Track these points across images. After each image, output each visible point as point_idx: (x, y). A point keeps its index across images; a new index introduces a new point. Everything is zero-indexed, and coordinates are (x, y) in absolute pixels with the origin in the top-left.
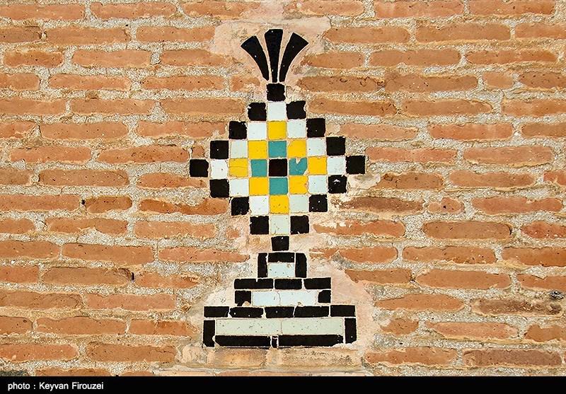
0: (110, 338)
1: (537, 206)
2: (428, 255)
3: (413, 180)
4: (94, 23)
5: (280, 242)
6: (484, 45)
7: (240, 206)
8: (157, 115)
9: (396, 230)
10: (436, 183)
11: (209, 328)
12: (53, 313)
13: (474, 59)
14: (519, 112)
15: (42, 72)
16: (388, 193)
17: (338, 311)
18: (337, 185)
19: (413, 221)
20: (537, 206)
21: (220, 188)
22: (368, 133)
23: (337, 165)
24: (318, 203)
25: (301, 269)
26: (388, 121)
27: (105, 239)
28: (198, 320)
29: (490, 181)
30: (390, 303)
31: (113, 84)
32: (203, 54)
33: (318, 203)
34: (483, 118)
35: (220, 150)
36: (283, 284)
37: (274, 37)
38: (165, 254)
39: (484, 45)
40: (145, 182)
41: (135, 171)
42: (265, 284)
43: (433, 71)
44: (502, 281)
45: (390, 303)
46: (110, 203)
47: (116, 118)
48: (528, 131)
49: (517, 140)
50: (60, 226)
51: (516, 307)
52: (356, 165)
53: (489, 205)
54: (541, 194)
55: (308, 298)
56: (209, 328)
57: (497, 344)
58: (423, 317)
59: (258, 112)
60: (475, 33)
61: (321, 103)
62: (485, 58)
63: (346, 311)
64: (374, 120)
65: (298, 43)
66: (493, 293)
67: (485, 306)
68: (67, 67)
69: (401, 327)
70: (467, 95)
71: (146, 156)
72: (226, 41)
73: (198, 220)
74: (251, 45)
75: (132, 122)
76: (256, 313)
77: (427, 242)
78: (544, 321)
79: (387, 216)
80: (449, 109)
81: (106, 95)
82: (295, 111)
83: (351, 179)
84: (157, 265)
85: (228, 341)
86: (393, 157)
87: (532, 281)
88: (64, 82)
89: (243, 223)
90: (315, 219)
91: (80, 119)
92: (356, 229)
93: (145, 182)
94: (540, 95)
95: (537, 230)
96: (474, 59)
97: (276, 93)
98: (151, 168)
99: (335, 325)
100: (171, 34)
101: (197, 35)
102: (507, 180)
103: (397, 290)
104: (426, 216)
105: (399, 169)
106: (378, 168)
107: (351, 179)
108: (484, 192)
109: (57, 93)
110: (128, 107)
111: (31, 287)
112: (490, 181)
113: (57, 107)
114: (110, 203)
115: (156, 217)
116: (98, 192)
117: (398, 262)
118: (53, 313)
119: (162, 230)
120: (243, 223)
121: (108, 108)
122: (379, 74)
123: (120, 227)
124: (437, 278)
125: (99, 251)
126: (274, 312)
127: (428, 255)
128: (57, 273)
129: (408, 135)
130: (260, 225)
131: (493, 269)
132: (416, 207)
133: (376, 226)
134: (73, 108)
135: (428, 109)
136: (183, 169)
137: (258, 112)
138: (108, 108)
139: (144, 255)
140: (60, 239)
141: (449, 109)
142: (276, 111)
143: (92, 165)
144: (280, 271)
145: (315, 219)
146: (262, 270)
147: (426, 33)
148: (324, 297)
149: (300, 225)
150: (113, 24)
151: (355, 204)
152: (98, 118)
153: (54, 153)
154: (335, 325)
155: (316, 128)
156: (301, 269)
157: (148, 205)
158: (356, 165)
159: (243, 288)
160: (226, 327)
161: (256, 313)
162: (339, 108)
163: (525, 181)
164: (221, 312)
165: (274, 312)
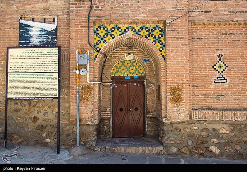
0: (206, 82)
1: (243, 70)
2: (233, 75)
3: (232, 68)
4: (203, 53)
5: (221, 74)
6: (238, 56)
7: (217, 70)
8: (209, 62)
9: (231, 72)
10: (234, 68)
11: (214, 81)
12: (200, 80)
13: (237, 57)
14: (241, 62)
15: (199, 58)
16: (230, 69)
17: (226, 80)
18: (226, 68)
19: (232, 72)
20: (243, 70)
21: (215, 69)
22: (228, 64)
23: (225, 67)
24: (224, 70)
25: (222, 76)
26: (230, 62)
27: (205, 73)
28: (213, 81)
29: (238, 68)
30: (230, 79)
31: (205, 59)
32: (213, 56)
33: (224, 70)
34: (238, 62)
35: (215, 65)
36: (221, 77)
37: (220, 55)
38: (210, 75)
39: (238, 56)
40: (208, 68)
41: (207, 67)
42: (219, 77)
43: (234, 58)
44: (240, 77)
45: (230, 79)
46: (205, 70)
47: (205, 62)
48: (242, 63)
49: (241, 64)
50: (201, 72)
51: (241, 79)
52: (227, 67)
53: (239, 70)
54: (243, 69)
55: (223, 79)
56: (214, 81)
57: (239, 82)
58: (233, 80)
59: (218, 62)
60: (237, 54)
61: (224, 61)
62: (238, 57)
63: (227, 80)
64: (228, 62)
65: (222, 55)
66: (239, 78)
67: (238, 79)
68: (201, 57)
69: (231, 81)
70: (237, 60)
71: (208, 66)
72: (215, 55)
73: (213, 72)
74: (218, 56)
75: (207, 63)
76: (219, 80)
77: (233, 73)
78: (243, 80)
79: (230, 71)
80: (235, 61)
81: (204, 60)
82: (222, 62)
83: (227, 68)
84: (210, 76)
85: (216, 82)
86: (230, 66)
87: (242, 77)
88: (201, 59)
89: (217, 72)
90: (224, 71)
91: (202, 62)
92: (227, 72)
93: (208, 68)
94: (243, 60)
95: (243, 72)
96: (237, 57)
97: (220, 60)
98: (209, 67)
99: (226, 81)
100: (210, 54)
101: (212, 55)
102: (240, 68)
103: (230, 78)
104: (233, 71)
105: (231, 67)
106: (229, 67)
107: (227, 68)
108: (238, 69)
109: (200, 60)
110: (207, 61)
111: (198, 78)
112: (238, 68)
113: (200, 61)
114: (205, 70)
115: (209, 71)
116: (204, 69)
117: (231, 75)
118: (200, 80)
119: (210, 73)
120: (217, 72)
121: (204, 61)
122: (229, 58)
123: (206, 72)
124: (234, 77)
125: (204, 75)
126: (220, 80)
127: (233, 75)
128: (201, 77)
129: (232, 64)
130: (219, 72)
131: (239, 76)
132: (232, 70)
133: (229, 72)
134: (202, 61)
135: (233, 61)
136: (212, 67)
137: (218, 62)
138: (204, 61)
139: (208, 75)
140: (201, 73)
141: (235, 61)
142: (220, 62)
143: (204, 67)
144: (220, 76)
145: (224, 71)
146: (219, 76)
147: (233, 54)
148: (224, 78)
149: (222, 72)
150: (205, 53)
151: (227, 70)
152: (204, 62)
153: (200, 66)
154: (226, 81)
155: (224, 63)
156: (222, 76)
157: (209, 70)
158: (227, 67)
159: (217, 78)
160: (216, 81)
161: (219, 80)
162: (225, 61)
163: (242, 68)
164: (215, 80)
165: (220, 80)
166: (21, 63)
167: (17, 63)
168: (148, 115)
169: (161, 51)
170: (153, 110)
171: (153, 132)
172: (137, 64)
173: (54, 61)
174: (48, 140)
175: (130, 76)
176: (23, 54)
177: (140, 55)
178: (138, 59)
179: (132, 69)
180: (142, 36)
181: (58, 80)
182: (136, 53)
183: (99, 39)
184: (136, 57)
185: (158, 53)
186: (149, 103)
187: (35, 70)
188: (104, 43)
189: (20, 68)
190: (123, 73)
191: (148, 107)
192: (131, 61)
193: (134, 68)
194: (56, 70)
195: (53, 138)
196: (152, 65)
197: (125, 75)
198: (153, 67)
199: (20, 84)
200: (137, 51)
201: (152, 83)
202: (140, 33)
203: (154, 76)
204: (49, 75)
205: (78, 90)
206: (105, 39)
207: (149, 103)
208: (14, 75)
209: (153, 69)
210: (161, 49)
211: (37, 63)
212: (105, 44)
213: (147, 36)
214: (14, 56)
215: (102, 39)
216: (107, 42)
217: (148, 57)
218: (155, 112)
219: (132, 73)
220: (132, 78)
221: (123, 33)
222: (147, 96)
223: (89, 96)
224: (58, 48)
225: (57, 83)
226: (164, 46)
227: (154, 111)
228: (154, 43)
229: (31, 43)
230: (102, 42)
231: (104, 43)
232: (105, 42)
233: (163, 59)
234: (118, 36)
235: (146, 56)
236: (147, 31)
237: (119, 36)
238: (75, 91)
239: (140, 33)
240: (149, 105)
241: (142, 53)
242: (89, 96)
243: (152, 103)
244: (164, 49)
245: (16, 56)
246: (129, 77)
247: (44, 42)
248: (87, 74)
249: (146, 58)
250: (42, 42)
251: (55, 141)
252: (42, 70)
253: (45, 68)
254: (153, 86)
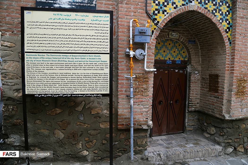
166: (46, 36)
167: (40, 36)
168: (191, 108)
169: (227, 32)
170: (196, 102)
171: (192, 127)
172: (179, 45)
173: (102, 35)
174: (85, 153)
175: (172, 60)
176: (51, 21)
177: (186, 35)
178: (184, 39)
179: (174, 52)
180: (209, 10)
181: (109, 67)
182: (181, 32)
183: (157, 7)
184: (181, 36)
185: (225, 35)
186: (193, 94)
187: (71, 49)
188: (163, 13)
189: (44, 45)
190: (164, 56)
191: (191, 99)
192: (173, 40)
193: (177, 50)
194: (106, 50)
195: (91, 149)
196: (198, 48)
197: (166, 59)
198: (199, 51)
199: (46, 71)
200: (183, 29)
201: (196, 71)
202: (206, 6)
203: (199, 62)
204: (94, 57)
205: (132, 81)
206: (165, 8)
207: (193, 94)
208: (35, 57)
209: (199, 53)
210: (228, 30)
211: (74, 37)
212: (165, 15)
213: (214, 12)
214: (35, 24)
215: (161, 8)
216: (167, 13)
217: (194, 38)
218: (198, 104)
219: (175, 56)
220: (174, 62)
221: (187, 4)
222: (191, 86)
223: (145, 89)
224: (109, 15)
225: (107, 71)
226: (231, 26)
227: (198, 103)
228: (221, 21)
229: (55, 4)
230: (161, 12)
231: (163, 13)
232: (165, 13)
233: (229, 43)
234: (180, 6)
235: (192, 36)
236: (214, 5)
237: (183, 7)
238: (125, 82)
239: (206, 6)
240: (193, 96)
241: (187, 32)
242: (145, 89)
243: (196, 94)
244: (231, 30)
245: (37, 24)
246: (171, 61)
247: (77, 4)
248: (144, 59)
249: (192, 38)
250: (73, 4)
251: (95, 153)
252: (82, 49)
253: (88, 46)
254: (198, 74)
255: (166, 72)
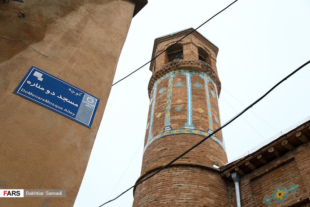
255: (58, 96)
